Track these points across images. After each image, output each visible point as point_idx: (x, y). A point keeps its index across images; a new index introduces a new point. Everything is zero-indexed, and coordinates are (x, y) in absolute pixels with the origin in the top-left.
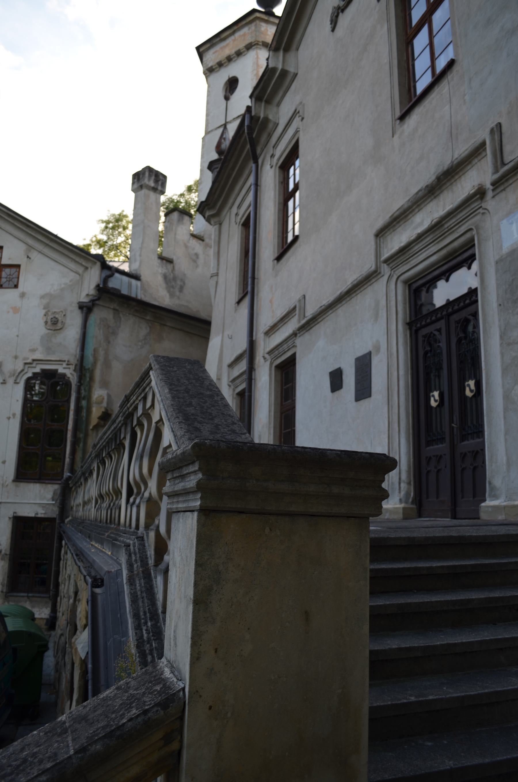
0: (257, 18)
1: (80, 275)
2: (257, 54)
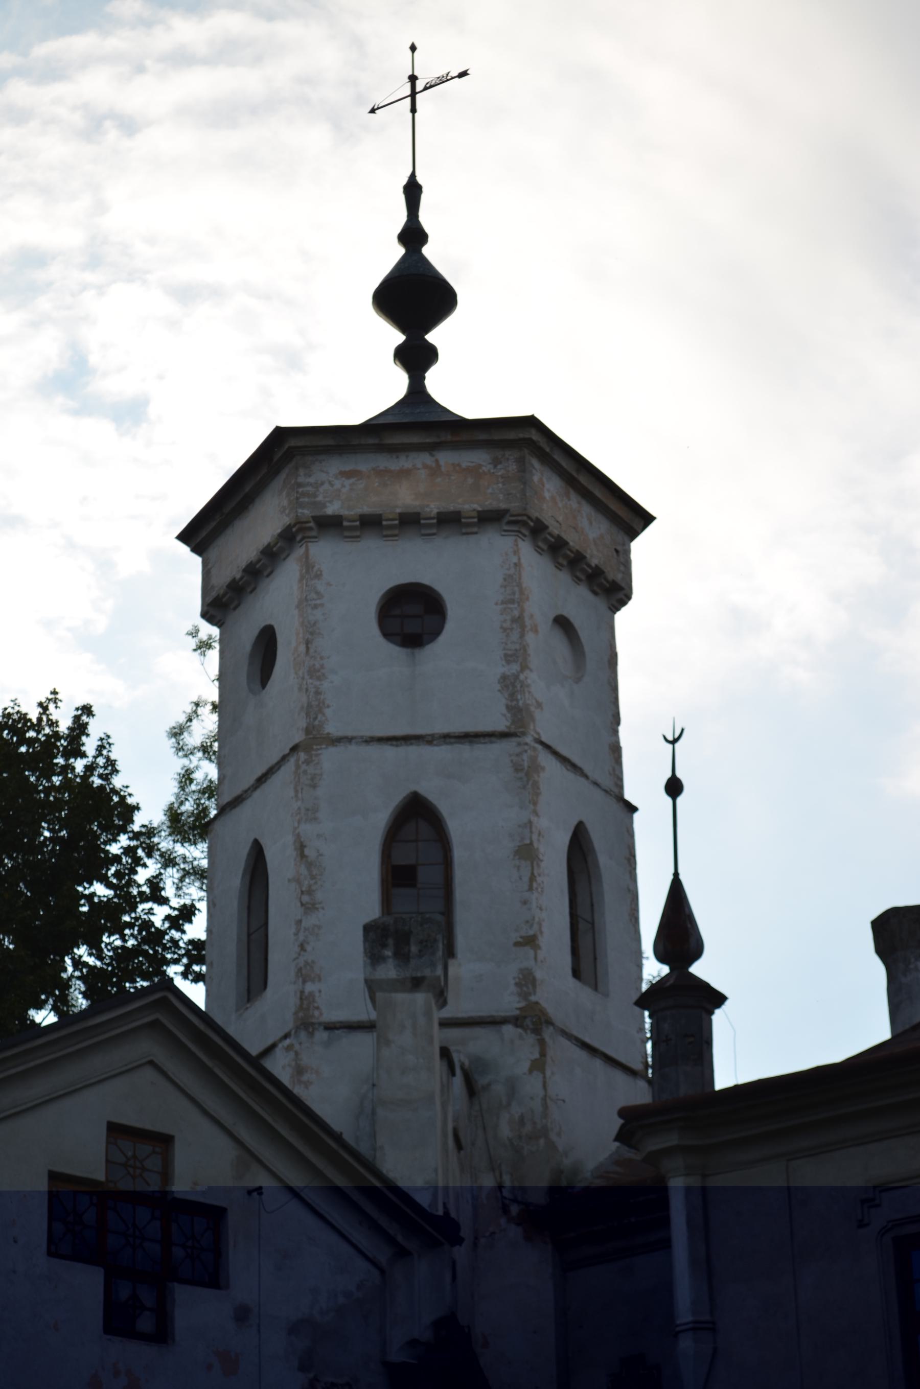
0: (530, 443)
1: (382, 1271)
2: (516, 552)
